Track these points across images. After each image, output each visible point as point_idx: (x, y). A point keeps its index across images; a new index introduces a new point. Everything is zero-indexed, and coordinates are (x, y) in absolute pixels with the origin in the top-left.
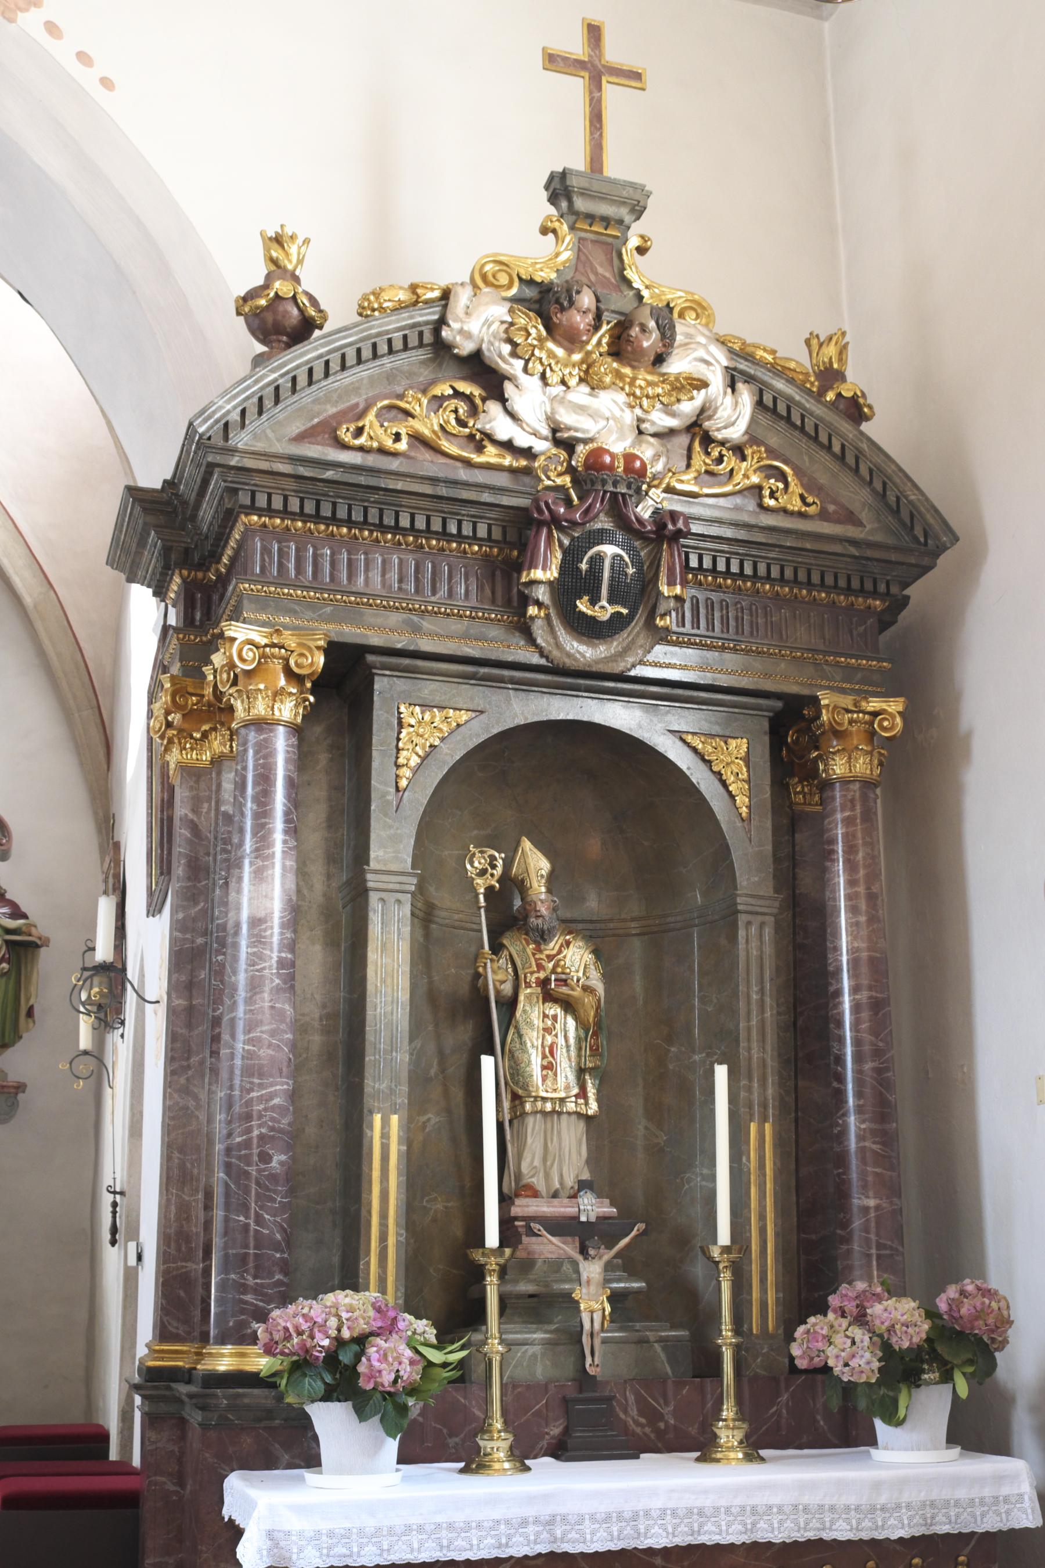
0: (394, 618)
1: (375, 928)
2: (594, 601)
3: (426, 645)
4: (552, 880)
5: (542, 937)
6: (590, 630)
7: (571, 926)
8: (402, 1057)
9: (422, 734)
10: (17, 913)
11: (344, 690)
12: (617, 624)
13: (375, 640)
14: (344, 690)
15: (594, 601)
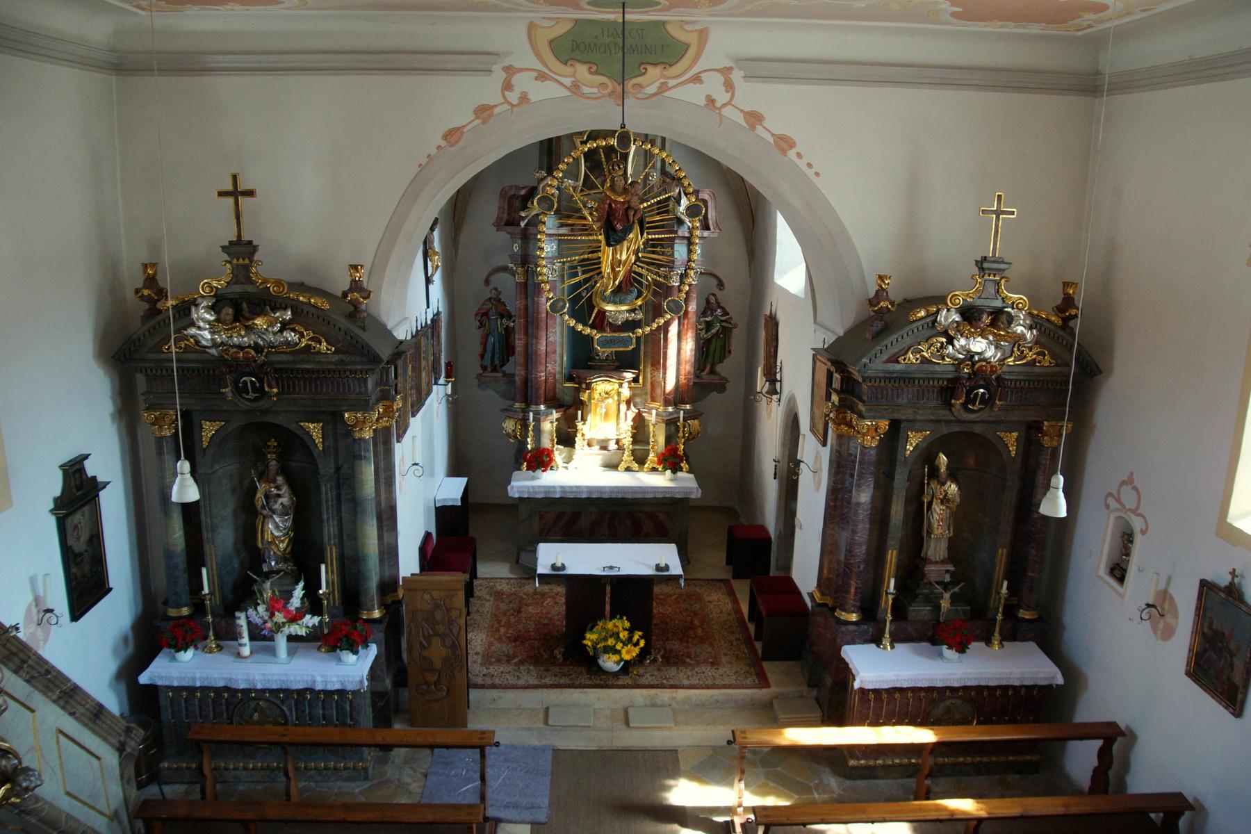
0: (910, 411)
1: (895, 498)
2: (974, 405)
3: (918, 417)
4: (948, 467)
5: (943, 484)
6: (972, 411)
7: (954, 479)
8: (899, 535)
9: (913, 442)
10: (725, 313)
11: (895, 433)
12: (981, 409)
13: (904, 418)
14: (895, 433)
15: (974, 405)
